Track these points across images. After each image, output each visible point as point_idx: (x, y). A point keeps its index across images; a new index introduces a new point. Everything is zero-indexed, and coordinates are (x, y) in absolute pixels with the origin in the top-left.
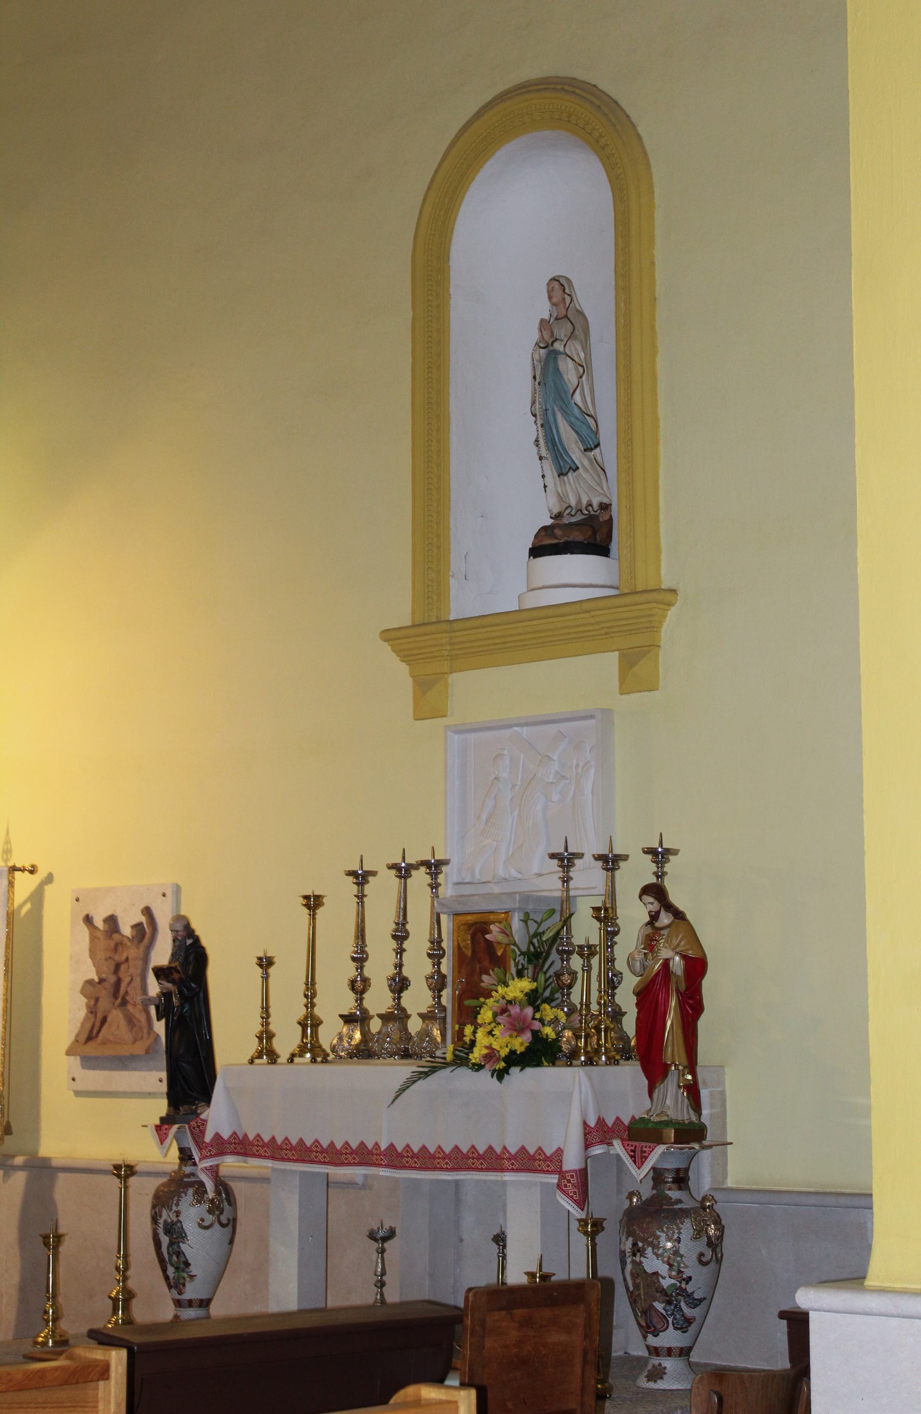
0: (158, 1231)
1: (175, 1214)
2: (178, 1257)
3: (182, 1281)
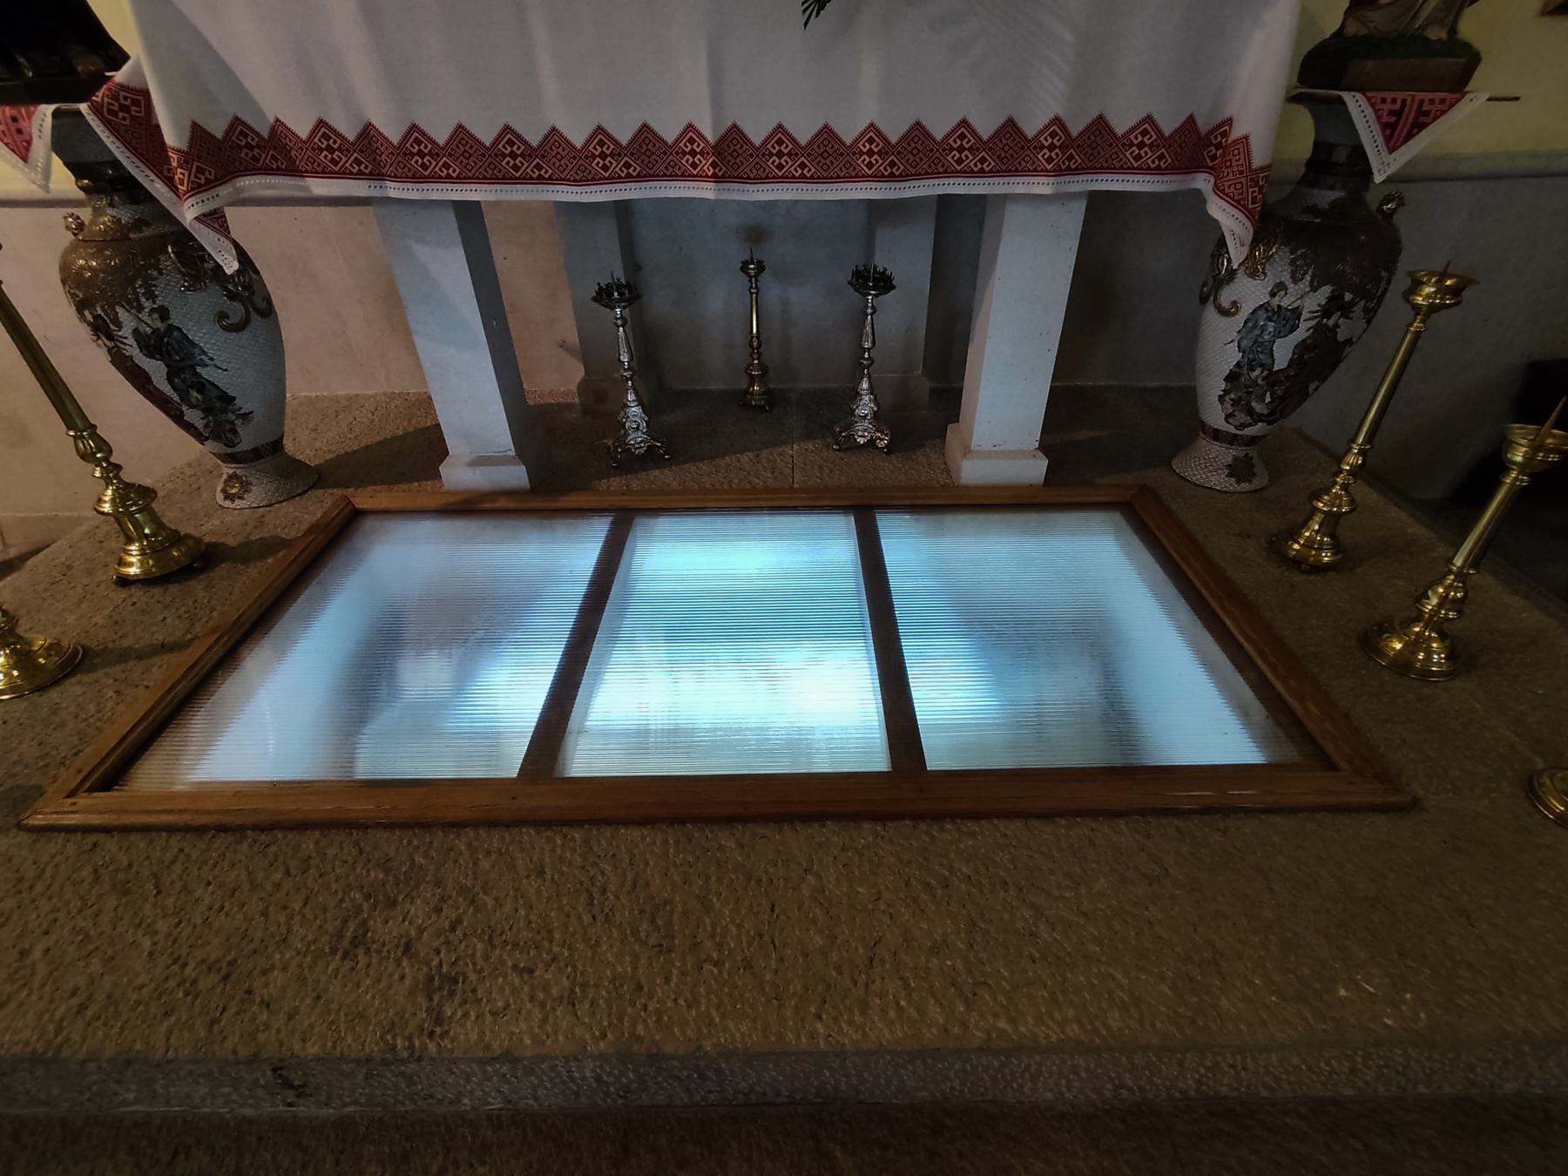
1: (156, 316)
3: (228, 427)
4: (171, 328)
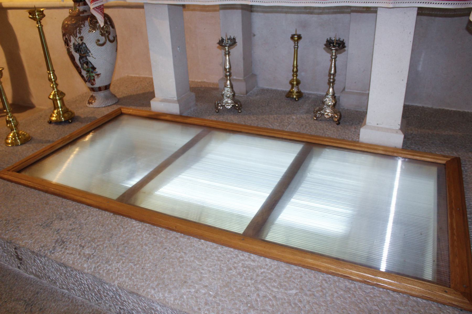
0: (71, 51)
1: (80, 39)
2: (87, 65)
3: (93, 78)
4: (83, 43)
